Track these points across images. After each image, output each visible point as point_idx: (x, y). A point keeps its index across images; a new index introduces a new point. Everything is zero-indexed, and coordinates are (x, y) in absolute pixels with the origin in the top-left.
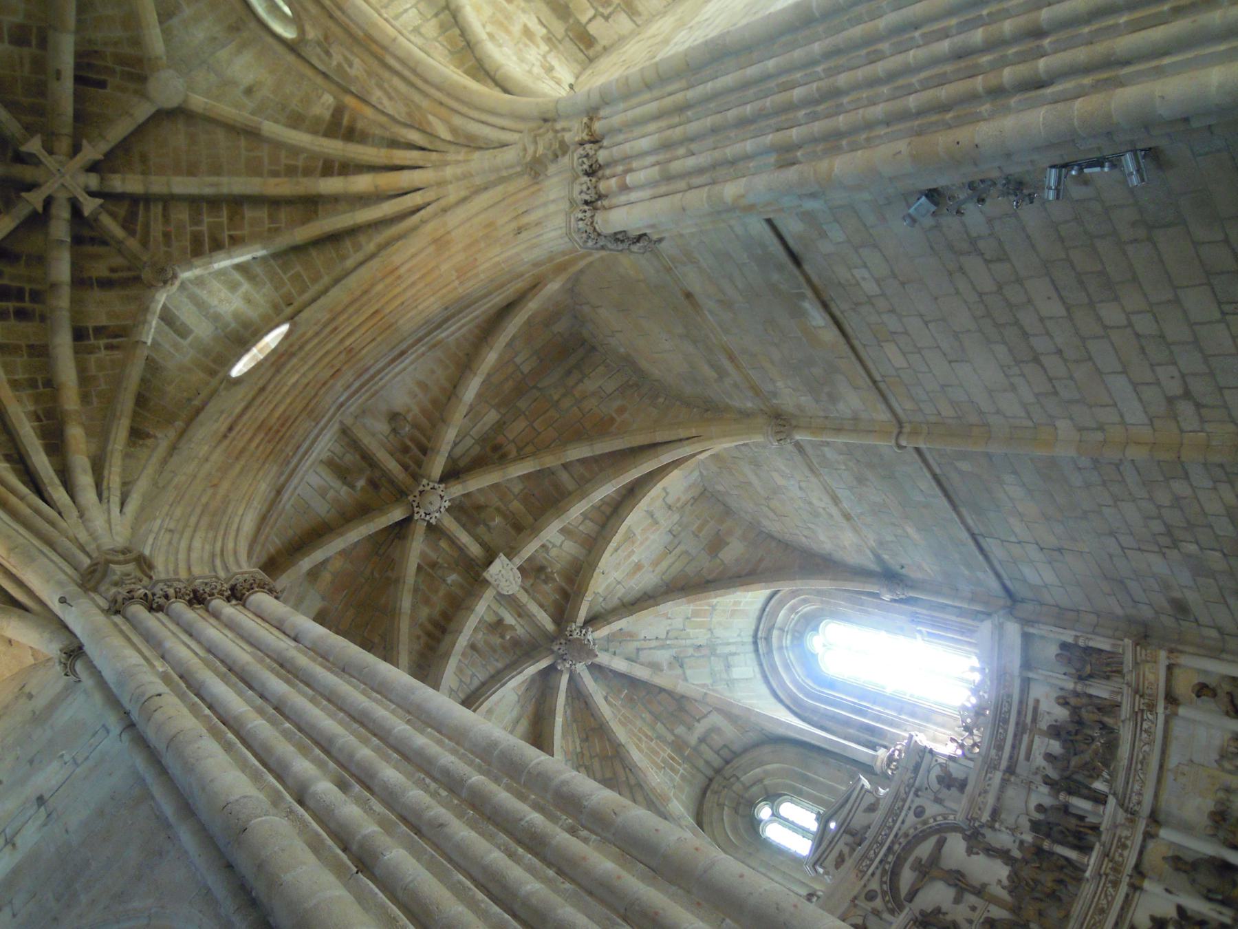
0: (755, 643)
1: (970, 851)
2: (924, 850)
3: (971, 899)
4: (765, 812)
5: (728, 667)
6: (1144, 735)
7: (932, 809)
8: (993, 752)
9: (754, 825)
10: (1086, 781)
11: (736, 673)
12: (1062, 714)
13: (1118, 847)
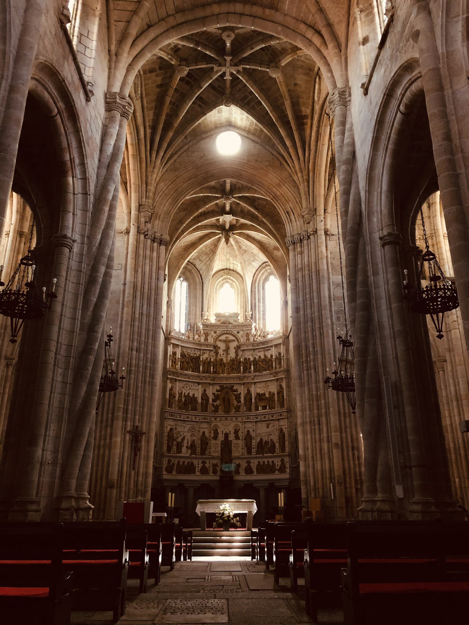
0: (264, 263)
1: (235, 348)
2: (231, 338)
3: (225, 353)
5: (254, 261)
7: (239, 335)
8: (256, 344)
11: (253, 263)
12: (269, 357)
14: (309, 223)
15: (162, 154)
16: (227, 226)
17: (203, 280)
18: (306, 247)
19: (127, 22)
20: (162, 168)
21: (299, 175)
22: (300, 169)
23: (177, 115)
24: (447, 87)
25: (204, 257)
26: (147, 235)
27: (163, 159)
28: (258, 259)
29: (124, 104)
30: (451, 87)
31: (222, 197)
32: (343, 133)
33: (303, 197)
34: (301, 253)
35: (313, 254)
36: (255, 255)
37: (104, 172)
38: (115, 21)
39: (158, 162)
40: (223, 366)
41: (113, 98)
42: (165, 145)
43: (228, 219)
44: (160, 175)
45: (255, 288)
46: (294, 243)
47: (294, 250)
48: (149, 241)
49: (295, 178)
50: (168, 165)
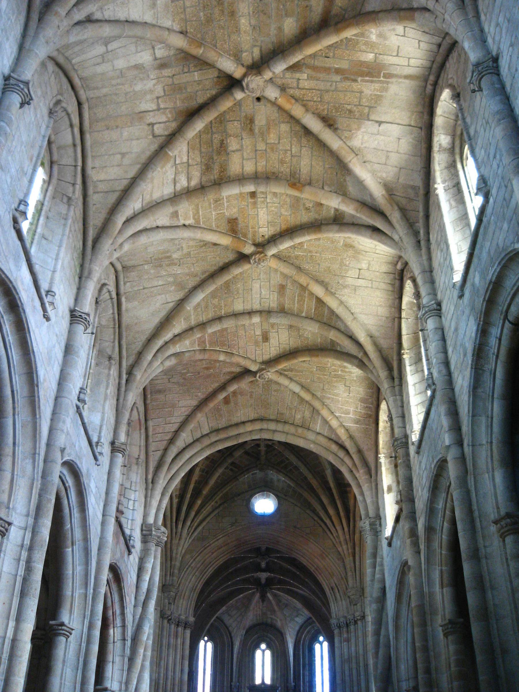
4: (263, 646)
5: (297, 616)
9: (257, 646)
14: (356, 605)
15: (188, 523)
16: (263, 581)
17: (233, 639)
18: (353, 634)
19: (164, 450)
20: (188, 538)
21: (345, 547)
22: (346, 540)
23: (206, 483)
24: (429, 623)
25: (234, 612)
26: (171, 619)
27: (190, 529)
28: (303, 614)
29: (159, 534)
30: (431, 625)
31: (257, 557)
32: (374, 567)
33: (349, 574)
34: (348, 640)
35: (361, 644)
36: (298, 610)
37: (140, 609)
38: (153, 451)
39: (185, 531)
41: (148, 531)
42: (193, 514)
43: (263, 576)
44: (186, 546)
45: (299, 651)
46: (339, 627)
47: (340, 634)
48: (173, 626)
49: (340, 549)
50: (195, 534)
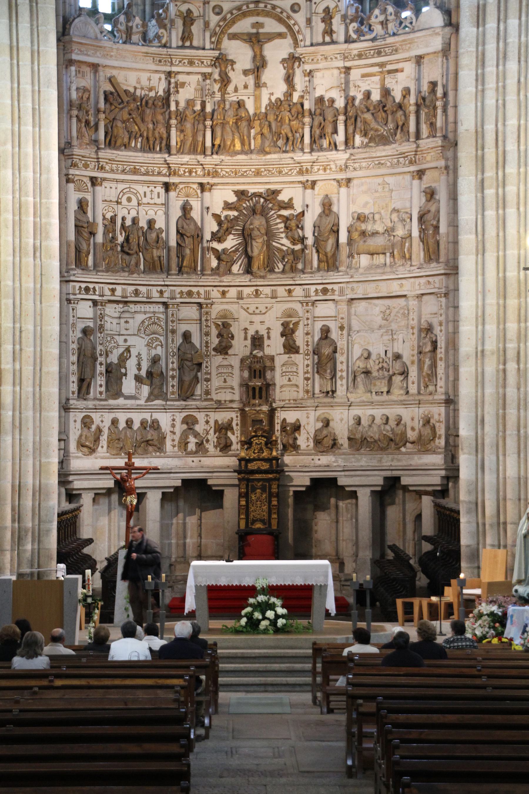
1: (284, 61)
6: (396, 160)
10: (358, 130)
13: (323, 166)
40: (243, 124)
